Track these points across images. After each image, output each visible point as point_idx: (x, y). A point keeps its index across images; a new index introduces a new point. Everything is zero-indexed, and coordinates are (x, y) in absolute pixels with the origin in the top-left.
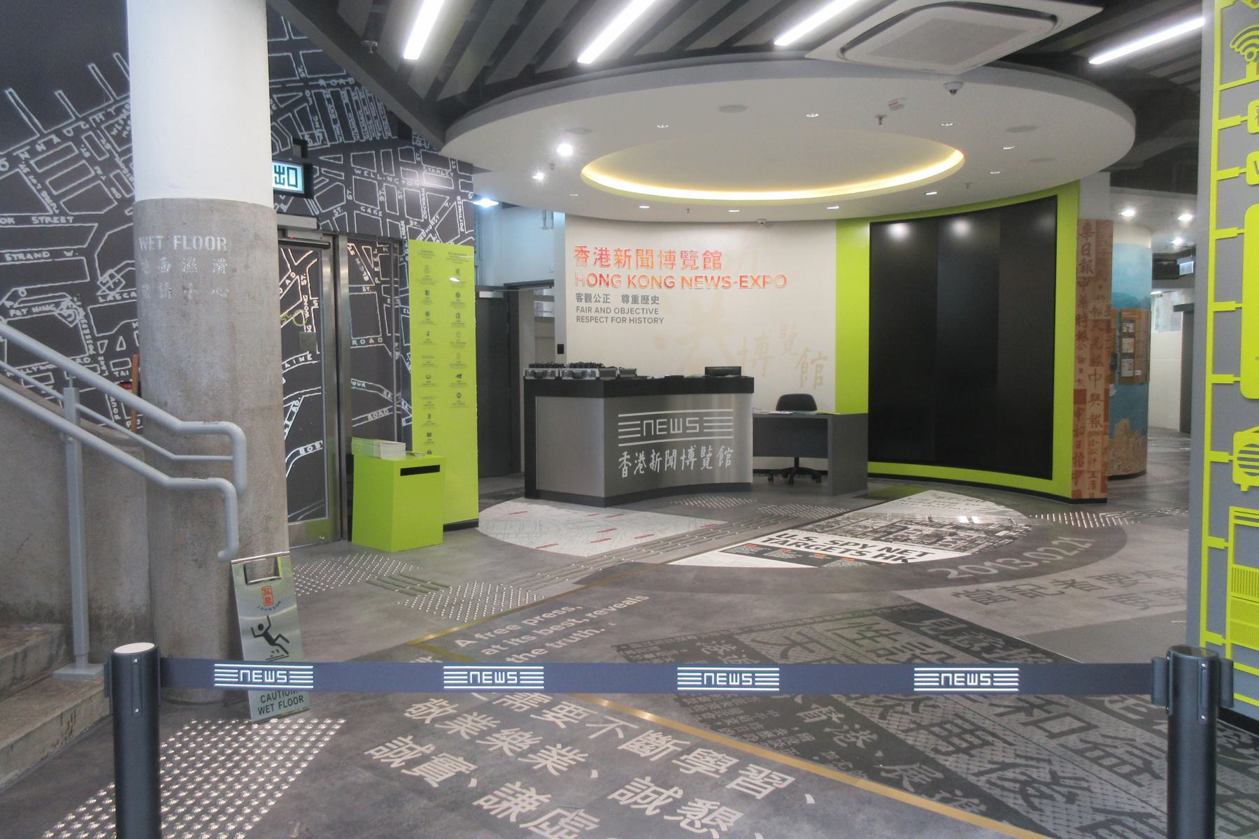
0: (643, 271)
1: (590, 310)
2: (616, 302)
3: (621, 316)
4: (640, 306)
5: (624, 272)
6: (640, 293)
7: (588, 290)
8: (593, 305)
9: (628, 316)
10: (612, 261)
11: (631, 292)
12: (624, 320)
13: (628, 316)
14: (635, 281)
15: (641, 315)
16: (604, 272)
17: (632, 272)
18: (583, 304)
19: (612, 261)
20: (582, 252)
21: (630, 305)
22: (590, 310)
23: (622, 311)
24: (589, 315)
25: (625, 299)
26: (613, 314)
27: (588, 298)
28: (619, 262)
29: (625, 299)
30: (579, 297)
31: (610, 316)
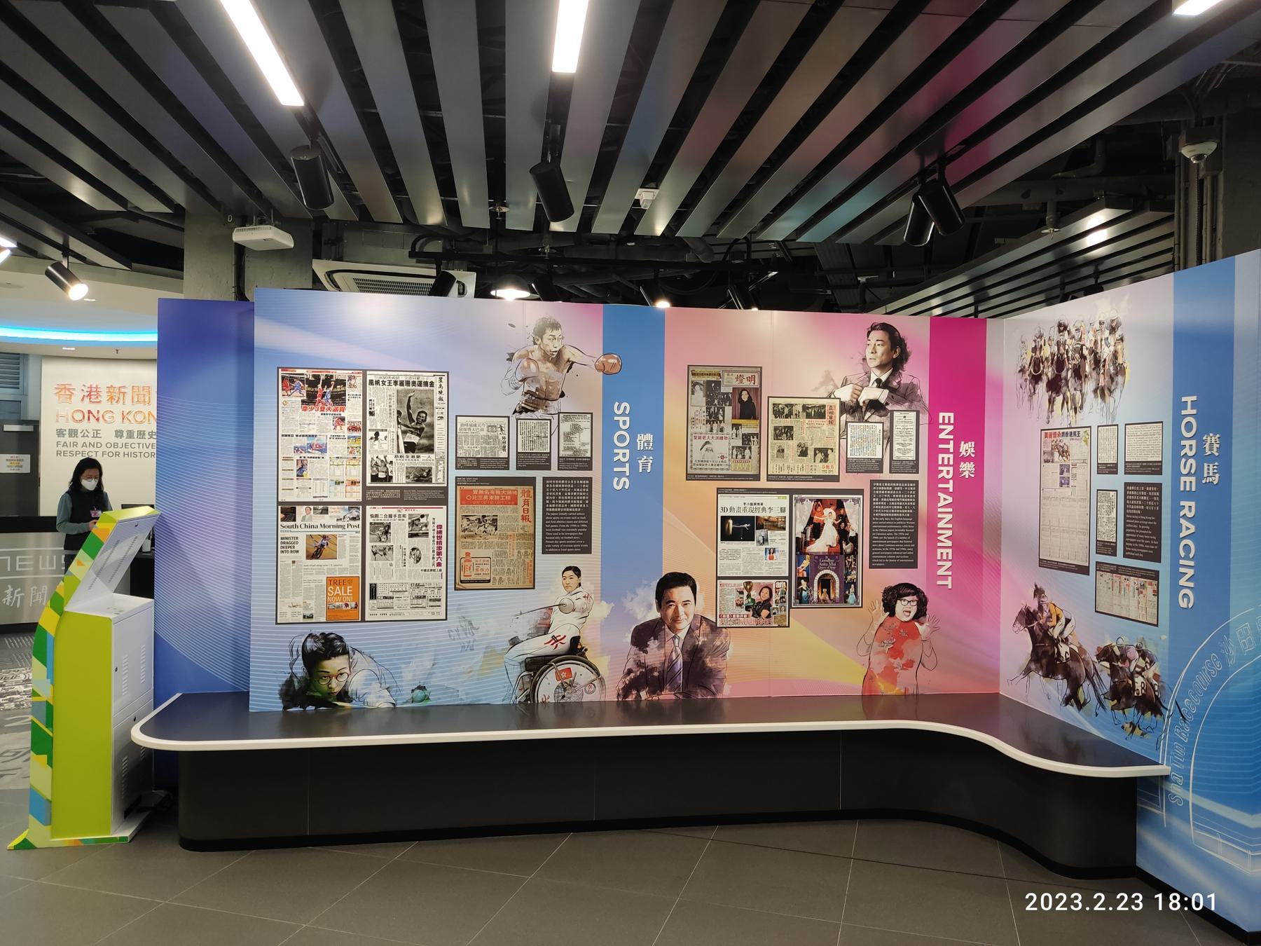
0: (139, 407)
1: (75, 444)
2: (107, 434)
3: (114, 450)
4: (136, 440)
5: (117, 408)
6: (136, 428)
7: (73, 426)
8: (80, 440)
9: (122, 451)
10: (104, 397)
11: (125, 427)
12: (117, 454)
13: (122, 451)
14: (131, 417)
15: (136, 450)
16: (94, 408)
17: (129, 406)
18: (67, 439)
19: (104, 397)
20: (65, 391)
21: (124, 440)
22: (75, 444)
23: (116, 445)
24: (75, 449)
25: (119, 434)
26: (104, 448)
27: (73, 433)
28: (112, 398)
29: (119, 434)
30: (60, 433)
31: (100, 450)
